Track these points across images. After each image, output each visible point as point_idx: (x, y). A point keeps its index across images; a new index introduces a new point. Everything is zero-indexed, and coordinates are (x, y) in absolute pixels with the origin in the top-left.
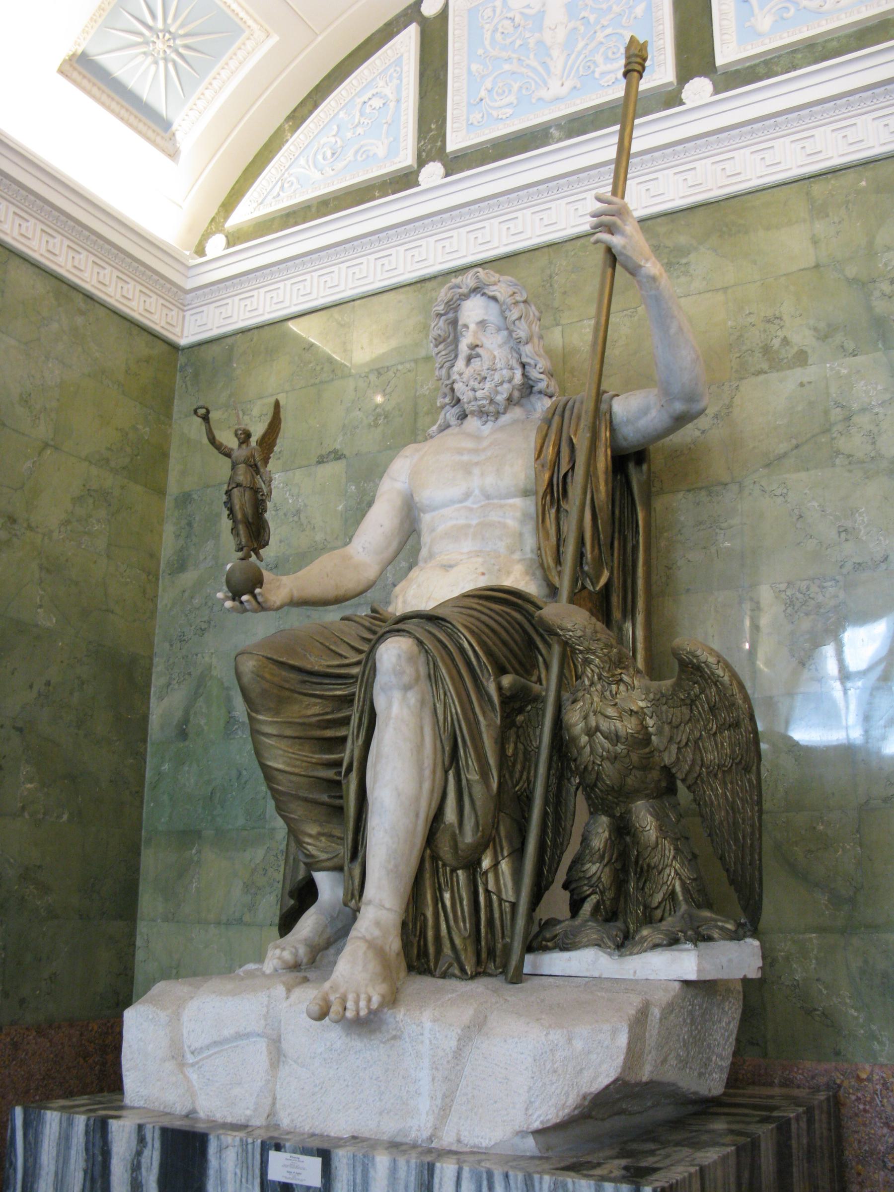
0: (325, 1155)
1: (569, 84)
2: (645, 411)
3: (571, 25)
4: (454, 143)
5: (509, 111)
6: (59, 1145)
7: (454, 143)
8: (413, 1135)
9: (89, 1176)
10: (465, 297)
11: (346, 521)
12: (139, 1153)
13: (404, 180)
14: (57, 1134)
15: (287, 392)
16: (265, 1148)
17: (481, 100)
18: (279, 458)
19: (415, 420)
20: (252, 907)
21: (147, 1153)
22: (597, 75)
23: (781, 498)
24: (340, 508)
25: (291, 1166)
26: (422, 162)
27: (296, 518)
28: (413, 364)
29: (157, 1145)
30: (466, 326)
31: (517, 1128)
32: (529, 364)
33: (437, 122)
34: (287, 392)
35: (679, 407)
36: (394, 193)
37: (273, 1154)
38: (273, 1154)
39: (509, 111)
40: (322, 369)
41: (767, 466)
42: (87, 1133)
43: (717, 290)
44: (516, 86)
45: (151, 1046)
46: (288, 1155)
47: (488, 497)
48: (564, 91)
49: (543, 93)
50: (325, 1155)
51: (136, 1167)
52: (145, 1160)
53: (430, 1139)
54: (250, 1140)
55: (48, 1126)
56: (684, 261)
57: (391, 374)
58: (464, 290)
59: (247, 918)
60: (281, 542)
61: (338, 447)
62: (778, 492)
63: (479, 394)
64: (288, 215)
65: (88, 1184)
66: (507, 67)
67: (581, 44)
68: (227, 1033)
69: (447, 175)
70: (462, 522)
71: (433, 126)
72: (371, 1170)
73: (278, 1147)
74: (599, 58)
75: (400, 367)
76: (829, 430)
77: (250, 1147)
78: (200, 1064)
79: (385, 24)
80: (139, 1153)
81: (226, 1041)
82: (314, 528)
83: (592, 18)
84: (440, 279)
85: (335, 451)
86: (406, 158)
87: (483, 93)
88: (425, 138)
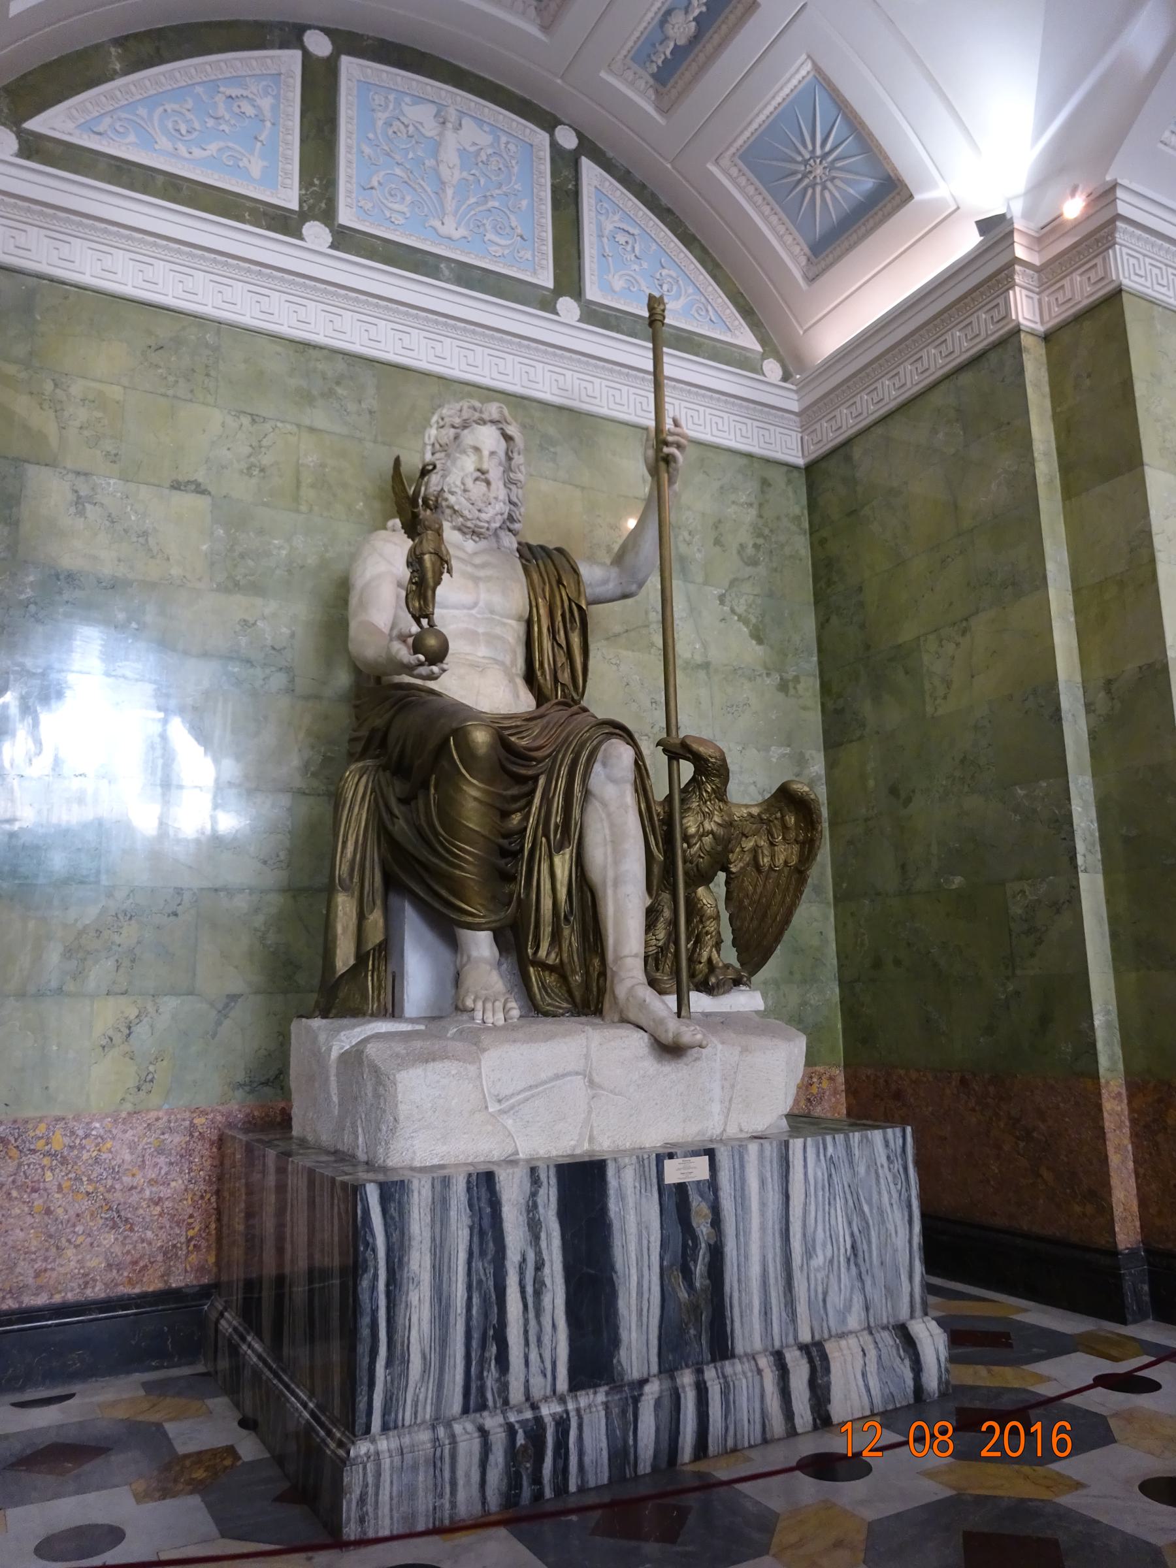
0: (711, 1153)
1: (462, 232)
2: (605, 582)
3: (465, 174)
4: (345, 217)
5: (402, 221)
6: (433, 1210)
7: (345, 217)
8: (709, 1133)
9: (476, 1231)
10: (483, 422)
11: (212, 564)
12: (534, 1194)
13: (285, 223)
14: (430, 1200)
15: (125, 387)
16: (660, 1159)
17: (372, 188)
18: (114, 462)
19: (298, 487)
20: (78, 975)
21: (542, 1192)
22: (486, 239)
23: (615, 667)
24: (204, 547)
25: (684, 1168)
26: (304, 216)
27: (141, 540)
28: (295, 429)
29: (553, 1181)
30: (477, 450)
31: (781, 1113)
32: (514, 504)
33: (321, 179)
34: (125, 387)
35: (634, 587)
36: (268, 228)
37: (667, 1162)
38: (667, 1162)
39: (402, 221)
40: (177, 382)
41: (607, 639)
42: (469, 1189)
43: (577, 486)
44: (408, 199)
45: (456, 1100)
46: (680, 1160)
47: (492, 612)
48: (457, 235)
49: (437, 223)
50: (711, 1153)
51: (532, 1207)
52: (541, 1199)
53: (722, 1133)
54: (646, 1156)
55: (416, 1194)
56: (552, 450)
57: (268, 426)
58: (486, 416)
59: (70, 987)
60: (119, 560)
61: (200, 480)
62: (614, 661)
63: (483, 516)
64: (119, 168)
65: (476, 1239)
66: (398, 171)
67: (472, 200)
68: (543, 1076)
69: (332, 246)
70: (471, 627)
71: (316, 182)
72: (746, 1157)
73: (671, 1156)
74: (488, 227)
75: (279, 424)
76: (647, 626)
77: (646, 1162)
78: (517, 1108)
79: (256, 22)
80: (534, 1194)
81: (545, 1082)
82: (168, 559)
83: (482, 181)
84: (325, 352)
85: (198, 485)
86: (289, 198)
87: (375, 184)
88: (307, 190)
